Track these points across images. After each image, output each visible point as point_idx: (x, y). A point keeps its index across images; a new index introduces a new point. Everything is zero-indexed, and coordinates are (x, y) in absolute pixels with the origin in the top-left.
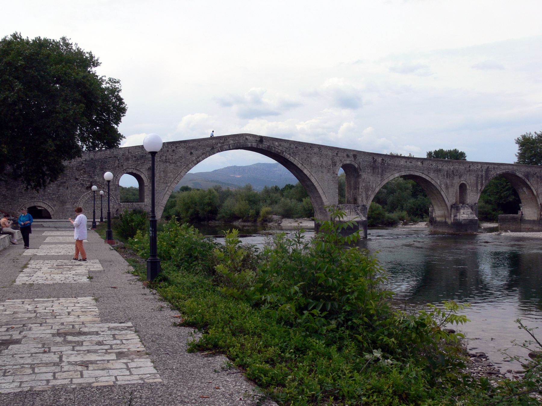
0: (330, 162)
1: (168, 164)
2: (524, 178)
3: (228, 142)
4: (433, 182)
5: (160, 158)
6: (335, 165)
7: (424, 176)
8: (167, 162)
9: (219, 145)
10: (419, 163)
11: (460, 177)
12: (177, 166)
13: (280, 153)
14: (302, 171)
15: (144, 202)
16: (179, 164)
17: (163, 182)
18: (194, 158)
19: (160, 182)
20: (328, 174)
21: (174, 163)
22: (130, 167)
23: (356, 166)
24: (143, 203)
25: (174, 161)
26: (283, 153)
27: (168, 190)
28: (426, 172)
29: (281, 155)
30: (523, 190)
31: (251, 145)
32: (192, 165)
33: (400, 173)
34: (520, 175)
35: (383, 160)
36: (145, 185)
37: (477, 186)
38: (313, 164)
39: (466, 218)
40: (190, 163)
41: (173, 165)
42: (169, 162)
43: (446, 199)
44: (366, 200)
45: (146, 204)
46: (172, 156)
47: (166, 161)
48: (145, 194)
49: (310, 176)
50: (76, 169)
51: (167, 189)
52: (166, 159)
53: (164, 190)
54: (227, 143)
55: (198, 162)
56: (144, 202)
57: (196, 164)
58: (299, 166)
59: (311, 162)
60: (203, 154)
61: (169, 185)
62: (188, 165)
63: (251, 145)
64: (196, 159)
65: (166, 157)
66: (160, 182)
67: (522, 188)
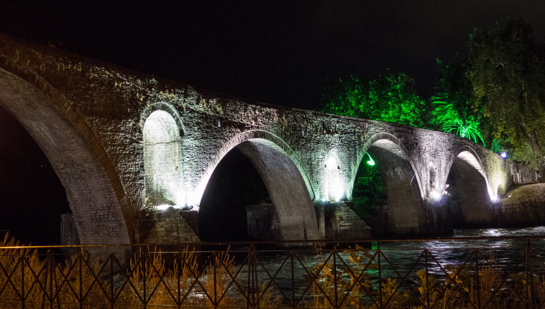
30: (394, 172)
67: (394, 169)
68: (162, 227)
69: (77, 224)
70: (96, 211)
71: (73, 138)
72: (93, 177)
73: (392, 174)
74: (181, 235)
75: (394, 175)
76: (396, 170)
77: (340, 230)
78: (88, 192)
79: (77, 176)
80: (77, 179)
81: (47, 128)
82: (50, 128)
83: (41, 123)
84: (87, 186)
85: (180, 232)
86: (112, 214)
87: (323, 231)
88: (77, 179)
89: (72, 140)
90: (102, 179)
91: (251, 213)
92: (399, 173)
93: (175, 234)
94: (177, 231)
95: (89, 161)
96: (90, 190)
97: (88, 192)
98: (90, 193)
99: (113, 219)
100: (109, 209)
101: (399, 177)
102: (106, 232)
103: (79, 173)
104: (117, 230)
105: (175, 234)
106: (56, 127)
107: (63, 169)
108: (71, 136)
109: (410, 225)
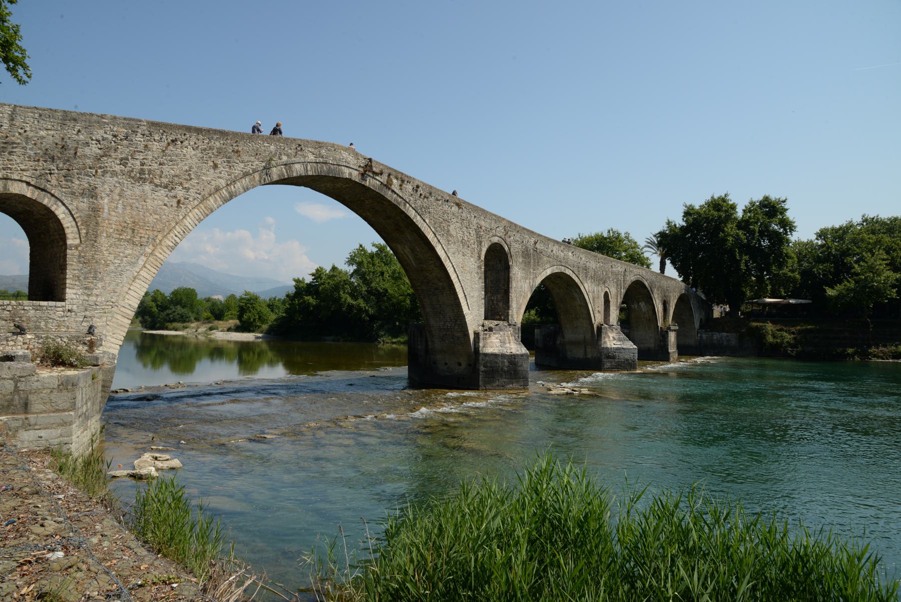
0: (473, 233)
1: (147, 187)
2: (649, 289)
3: (305, 157)
4: (582, 288)
5: (125, 165)
6: (481, 242)
7: (574, 277)
8: (145, 180)
9: (285, 158)
10: (570, 254)
11: (604, 283)
12: (175, 197)
13: (399, 203)
14: (432, 249)
15: (63, 300)
16: (180, 193)
17: (131, 241)
18: (222, 182)
19: (120, 240)
20: (472, 259)
21: (166, 187)
22: (15, 177)
23: (506, 248)
24: (59, 304)
25: (165, 181)
26: (405, 205)
27: (144, 266)
28: (575, 270)
29: (402, 208)
30: (638, 305)
31: (350, 174)
32: (216, 200)
33: (552, 268)
34: (646, 284)
35: (536, 243)
36: (69, 242)
37: (617, 299)
38: (451, 236)
39: (619, 346)
40: (210, 195)
41: (163, 192)
42: (151, 182)
43: (592, 315)
44: (517, 313)
45: (69, 307)
46: (160, 164)
47: (141, 177)
48: (69, 273)
49: (446, 261)
51: (141, 263)
52: (142, 172)
53: (133, 264)
54: (302, 160)
55: (232, 196)
56: (63, 300)
57: (226, 201)
58: (430, 236)
59: (448, 231)
60: (246, 174)
61: (148, 250)
62: (204, 199)
63: (350, 174)
64: (228, 185)
65: (142, 164)
66: (120, 240)
67: (638, 304)
68: (497, 338)
69: (427, 332)
70: (444, 322)
71: (431, 260)
72: (445, 295)
73: (636, 306)
74: (512, 346)
75: (638, 307)
76: (640, 303)
79: (431, 293)
81: (409, 250)
82: (413, 250)
83: (406, 246)
85: (512, 343)
89: (431, 262)
90: (452, 296)
91: (539, 330)
92: (642, 306)
93: (508, 345)
94: (510, 343)
95: (442, 280)
99: (459, 330)
100: (456, 321)
101: (641, 310)
102: (451, 340)
105: (508, 345)
106: (418, 250)
108: (430, 258)
109: (646, 345)
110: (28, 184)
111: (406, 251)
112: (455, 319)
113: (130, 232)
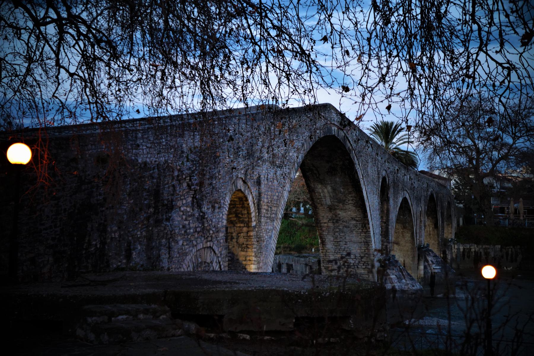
13: (350, 150)
50: (178, 176)
74: (408, 282)
77: (434, 272)
78: (344, 243)
80: (337, 232)
84: (345, 239)
86: (363, 262)
87: (422, 272)
88: (337, 232)
93: (404, 281)
96: (346, 242)
97: (344, 243)
98: (346, 244)
99: (364, 267)
103: (341, 227)
104: (364, 276)
107: (325, 223)
110: (242, 179)
111: (326, 190)
112: (360, 256)
113: (270, 209)
